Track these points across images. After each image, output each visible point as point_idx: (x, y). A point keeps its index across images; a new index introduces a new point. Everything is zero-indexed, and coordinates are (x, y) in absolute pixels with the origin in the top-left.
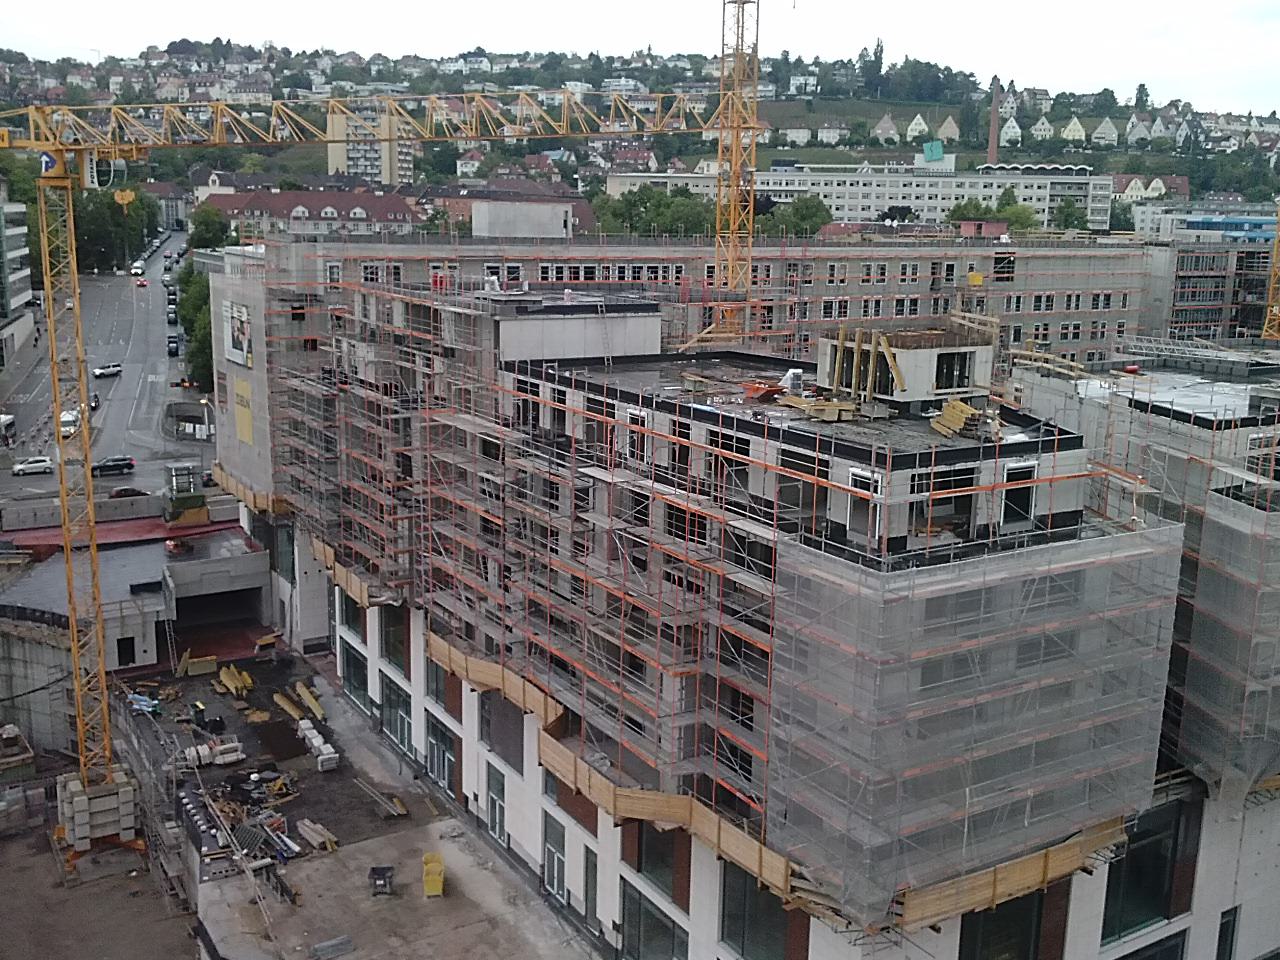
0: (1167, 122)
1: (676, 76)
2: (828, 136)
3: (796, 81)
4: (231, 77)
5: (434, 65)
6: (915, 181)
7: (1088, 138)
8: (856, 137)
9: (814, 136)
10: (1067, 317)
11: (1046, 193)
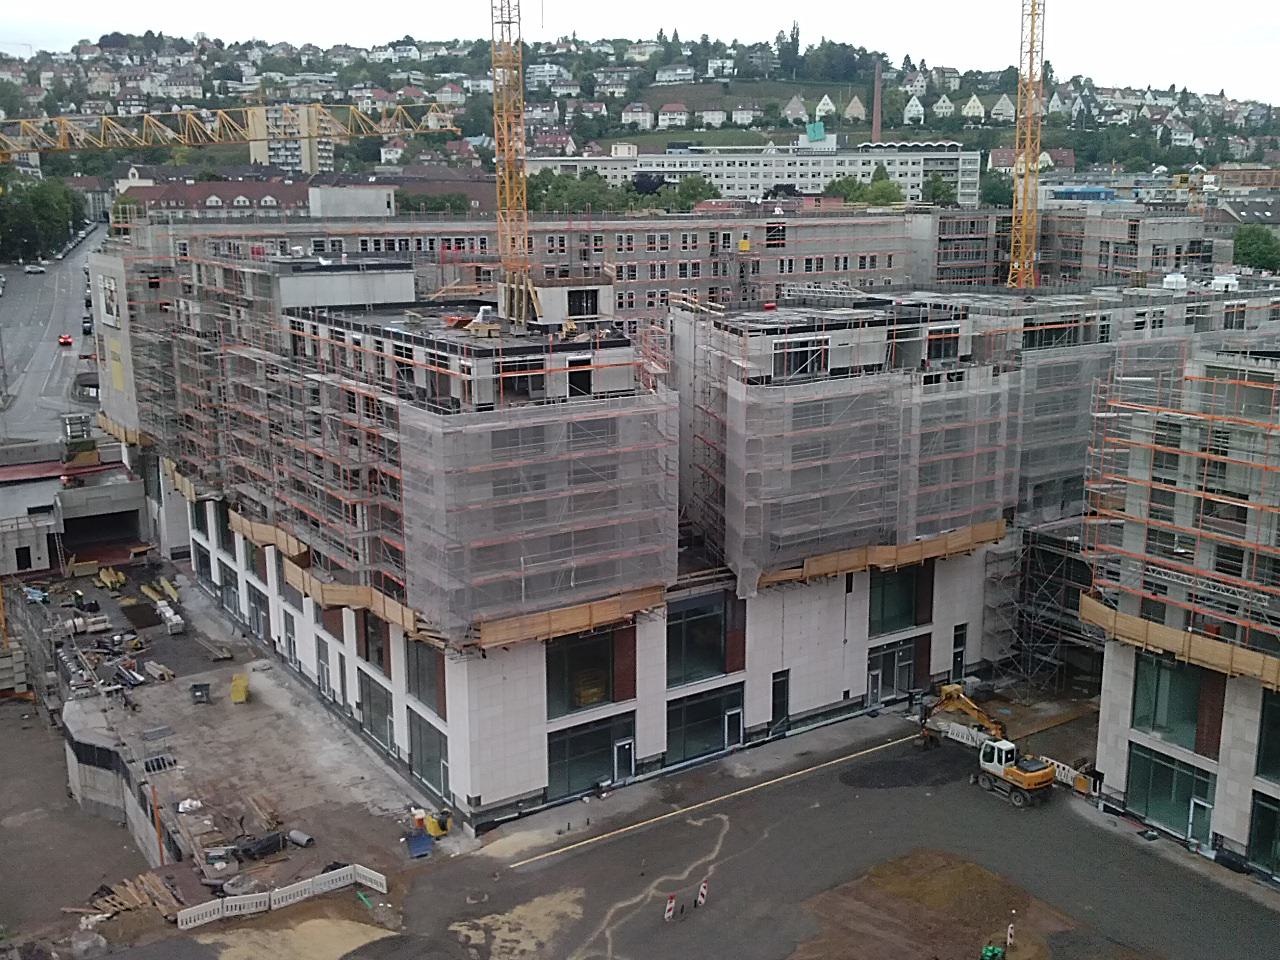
0: (1064, 98)
1: (600, 61)
2: (742, 117)
3: (714, 64)
4: (162, 69)
5: (363, 54)
6: (798, 160)
7: (988, 114)
8: (768, 118)
10: (836, 277)
11: (920, 168)
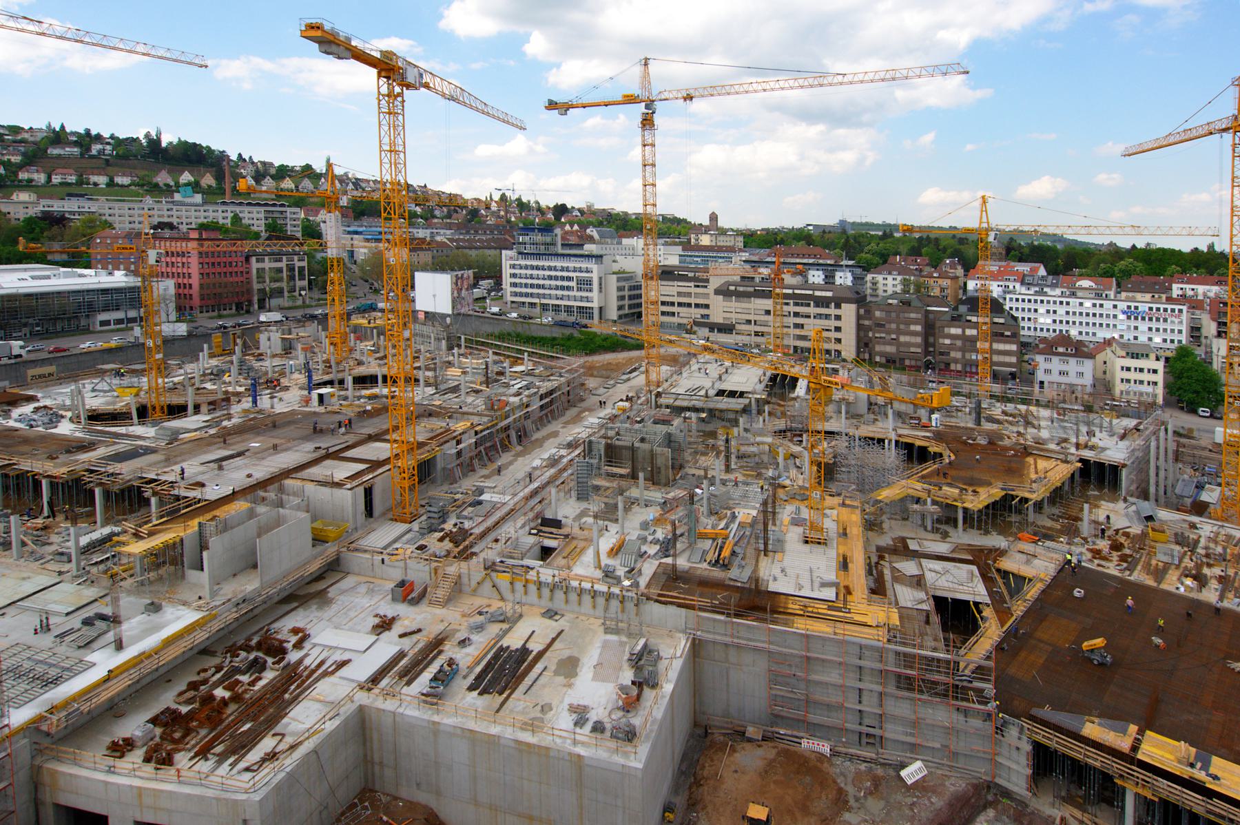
6: (175, 208)
7: (297, 187)
8: (141, 182)
9: (112, 180)
11: (262, 215)
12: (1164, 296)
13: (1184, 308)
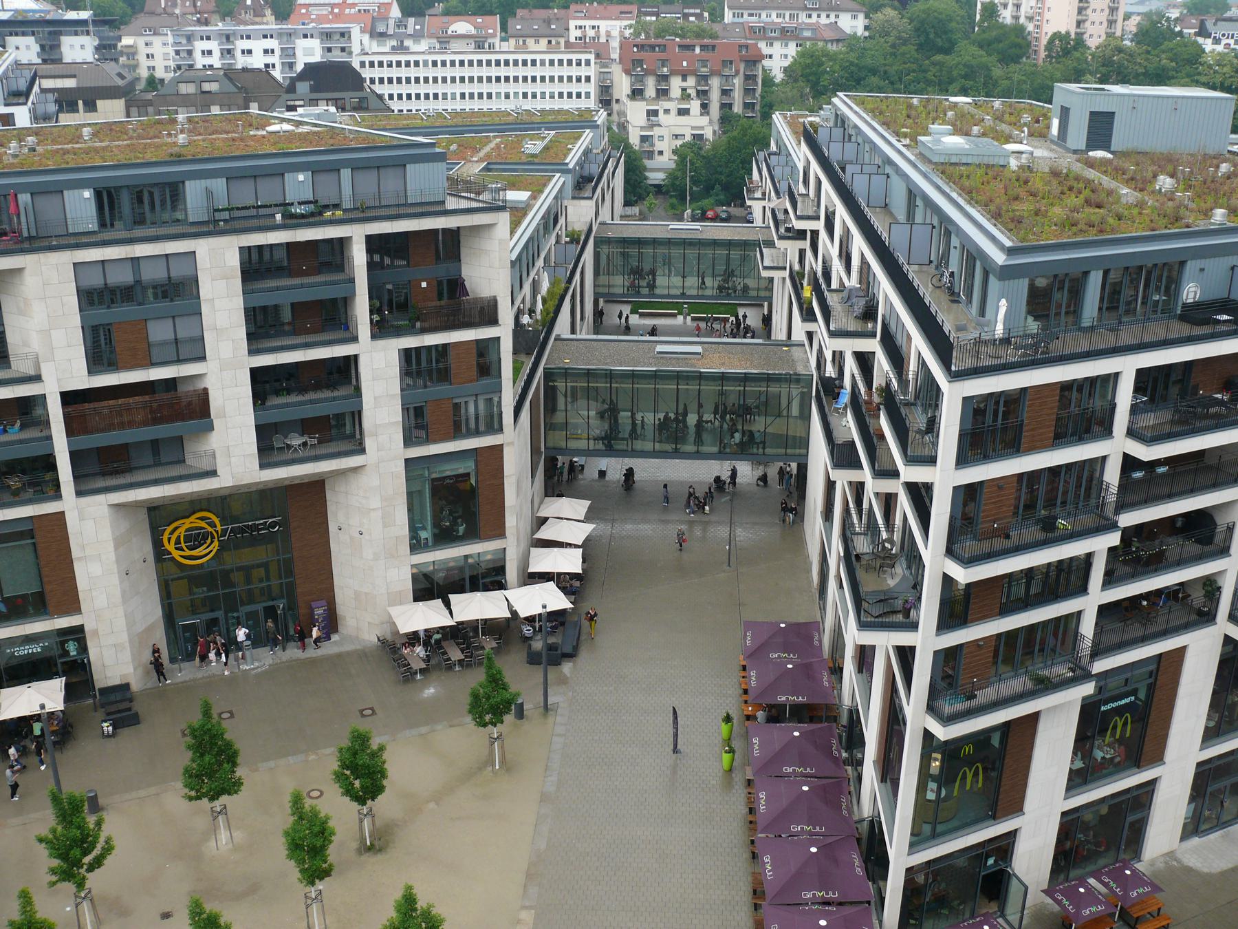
12: (562, 41)
13: (592, 57)
